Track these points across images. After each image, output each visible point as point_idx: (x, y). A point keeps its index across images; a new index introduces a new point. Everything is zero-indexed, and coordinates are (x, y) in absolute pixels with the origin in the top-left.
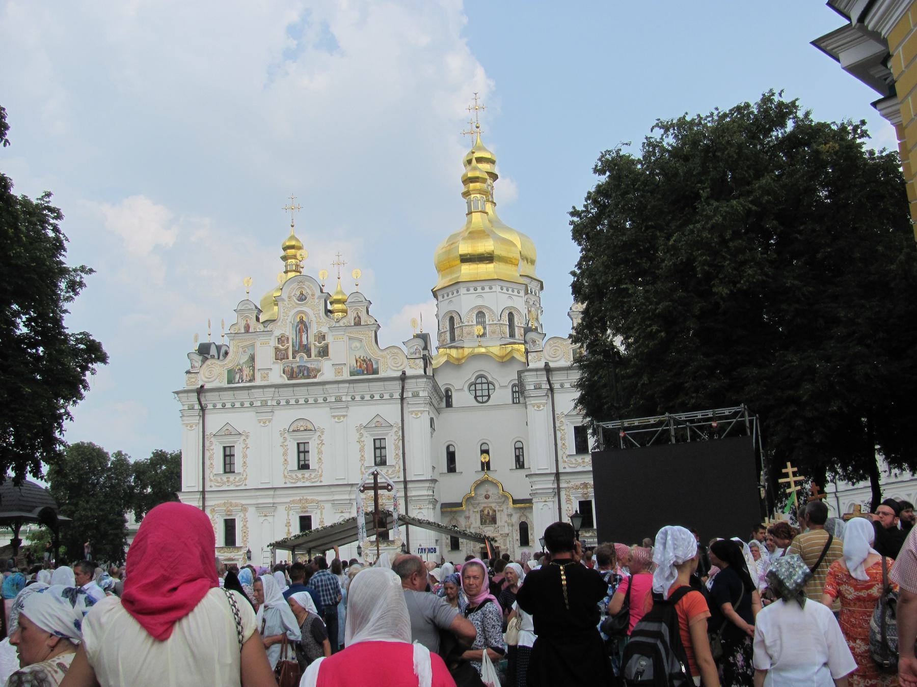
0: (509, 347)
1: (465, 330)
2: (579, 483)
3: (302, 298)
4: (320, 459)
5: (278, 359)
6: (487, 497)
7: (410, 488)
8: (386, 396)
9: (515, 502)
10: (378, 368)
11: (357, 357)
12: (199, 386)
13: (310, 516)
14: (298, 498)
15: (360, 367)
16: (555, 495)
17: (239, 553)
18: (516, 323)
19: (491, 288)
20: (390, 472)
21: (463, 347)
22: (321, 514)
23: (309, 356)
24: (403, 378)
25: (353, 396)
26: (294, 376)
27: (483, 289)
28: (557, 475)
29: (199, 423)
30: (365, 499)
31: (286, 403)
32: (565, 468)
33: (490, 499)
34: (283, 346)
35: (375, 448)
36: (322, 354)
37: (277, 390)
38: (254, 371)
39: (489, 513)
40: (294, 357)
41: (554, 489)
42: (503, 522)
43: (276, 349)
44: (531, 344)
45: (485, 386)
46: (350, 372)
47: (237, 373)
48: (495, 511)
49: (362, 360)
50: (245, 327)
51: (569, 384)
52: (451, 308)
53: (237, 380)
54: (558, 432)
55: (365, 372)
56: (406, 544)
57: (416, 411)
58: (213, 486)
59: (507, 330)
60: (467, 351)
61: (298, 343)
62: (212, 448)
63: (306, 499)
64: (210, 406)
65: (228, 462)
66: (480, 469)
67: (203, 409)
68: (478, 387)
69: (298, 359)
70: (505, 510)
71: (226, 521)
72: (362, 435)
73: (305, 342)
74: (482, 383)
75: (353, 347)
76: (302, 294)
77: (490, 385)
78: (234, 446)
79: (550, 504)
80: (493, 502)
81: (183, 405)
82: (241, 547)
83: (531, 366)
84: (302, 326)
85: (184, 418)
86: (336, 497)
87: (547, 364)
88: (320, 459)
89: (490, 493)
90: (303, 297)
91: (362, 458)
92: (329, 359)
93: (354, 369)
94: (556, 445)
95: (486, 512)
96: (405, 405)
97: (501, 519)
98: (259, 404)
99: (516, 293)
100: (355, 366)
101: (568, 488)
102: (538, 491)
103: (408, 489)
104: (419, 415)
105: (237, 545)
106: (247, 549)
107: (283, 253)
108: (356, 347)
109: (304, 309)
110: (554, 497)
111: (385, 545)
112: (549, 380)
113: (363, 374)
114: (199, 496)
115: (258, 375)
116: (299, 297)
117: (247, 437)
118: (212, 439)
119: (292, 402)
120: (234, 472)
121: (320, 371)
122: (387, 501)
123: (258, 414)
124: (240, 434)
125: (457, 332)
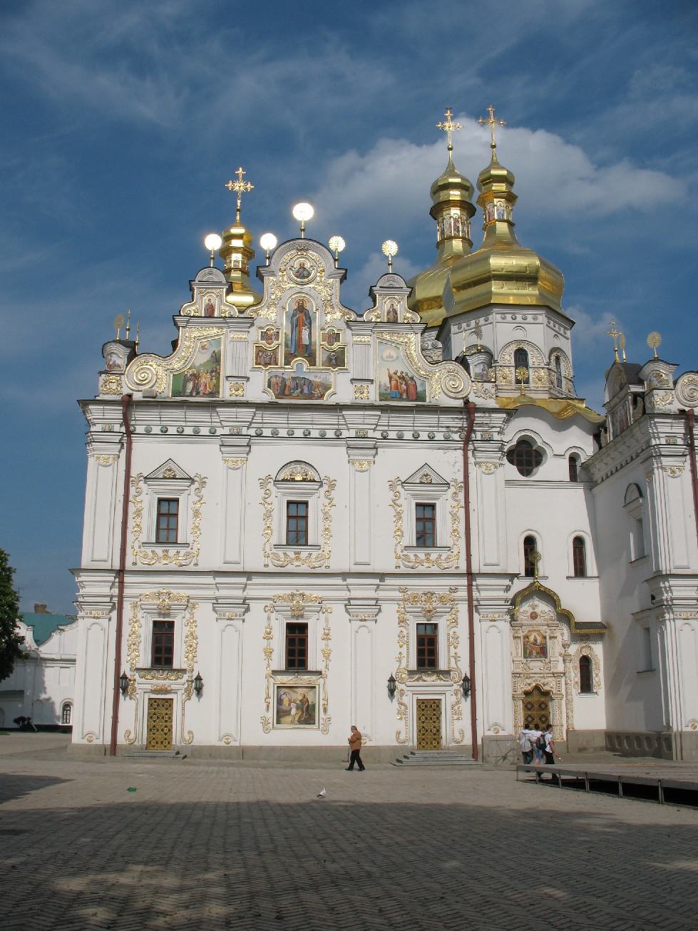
1: (499, 374)
5: (259, 364)
6: (534, 616)
10: (425, 391)
11: (392, 372)
13: (306, 625)
14: (289, 592)
15: (397, 388)
17: (179, 681)
22: (327, 620)
23: (313, 363)
24: (468, 409)
26: (287, 392)
29: (119, 457)
33: (538, 621)
36: (334, 361)
38: (218, 379)
39: (536, 640)
40: (288, 363)
42: (557, 654)
43: (260, 350)
46: (381, 394)
48: (545, 638)
49: (399, 377)
50: (206, 310)
55: (405, 397)
56: (469, 676)
59: (554, 378)
61: (294, 343)
62: (138, 499)
63: (303, 595)
64: (140, 429)
65: (163, 525)
67: (129, 433)
70: (560, 638)
71: (155, 623)
72: (397, 495)
73: (305, 341)
75: (385, 356)
76: (302, 267)
82: (184, 671)
84: (301, 316)
86: (354, 594)
88: (326, 529)
89: (538, 610)
91: (399, 533)
95: (532, 639)
96: (470, 453)
97: (555, 648)
98: (226, 431)
99: (562, 332)
105: (176, 665)
106: (195, 675)
108: (390, 357)
111: (434, 677)
113: (401, 399)
118: (142, 484)
121: (330, 388)
123: (223, 449)
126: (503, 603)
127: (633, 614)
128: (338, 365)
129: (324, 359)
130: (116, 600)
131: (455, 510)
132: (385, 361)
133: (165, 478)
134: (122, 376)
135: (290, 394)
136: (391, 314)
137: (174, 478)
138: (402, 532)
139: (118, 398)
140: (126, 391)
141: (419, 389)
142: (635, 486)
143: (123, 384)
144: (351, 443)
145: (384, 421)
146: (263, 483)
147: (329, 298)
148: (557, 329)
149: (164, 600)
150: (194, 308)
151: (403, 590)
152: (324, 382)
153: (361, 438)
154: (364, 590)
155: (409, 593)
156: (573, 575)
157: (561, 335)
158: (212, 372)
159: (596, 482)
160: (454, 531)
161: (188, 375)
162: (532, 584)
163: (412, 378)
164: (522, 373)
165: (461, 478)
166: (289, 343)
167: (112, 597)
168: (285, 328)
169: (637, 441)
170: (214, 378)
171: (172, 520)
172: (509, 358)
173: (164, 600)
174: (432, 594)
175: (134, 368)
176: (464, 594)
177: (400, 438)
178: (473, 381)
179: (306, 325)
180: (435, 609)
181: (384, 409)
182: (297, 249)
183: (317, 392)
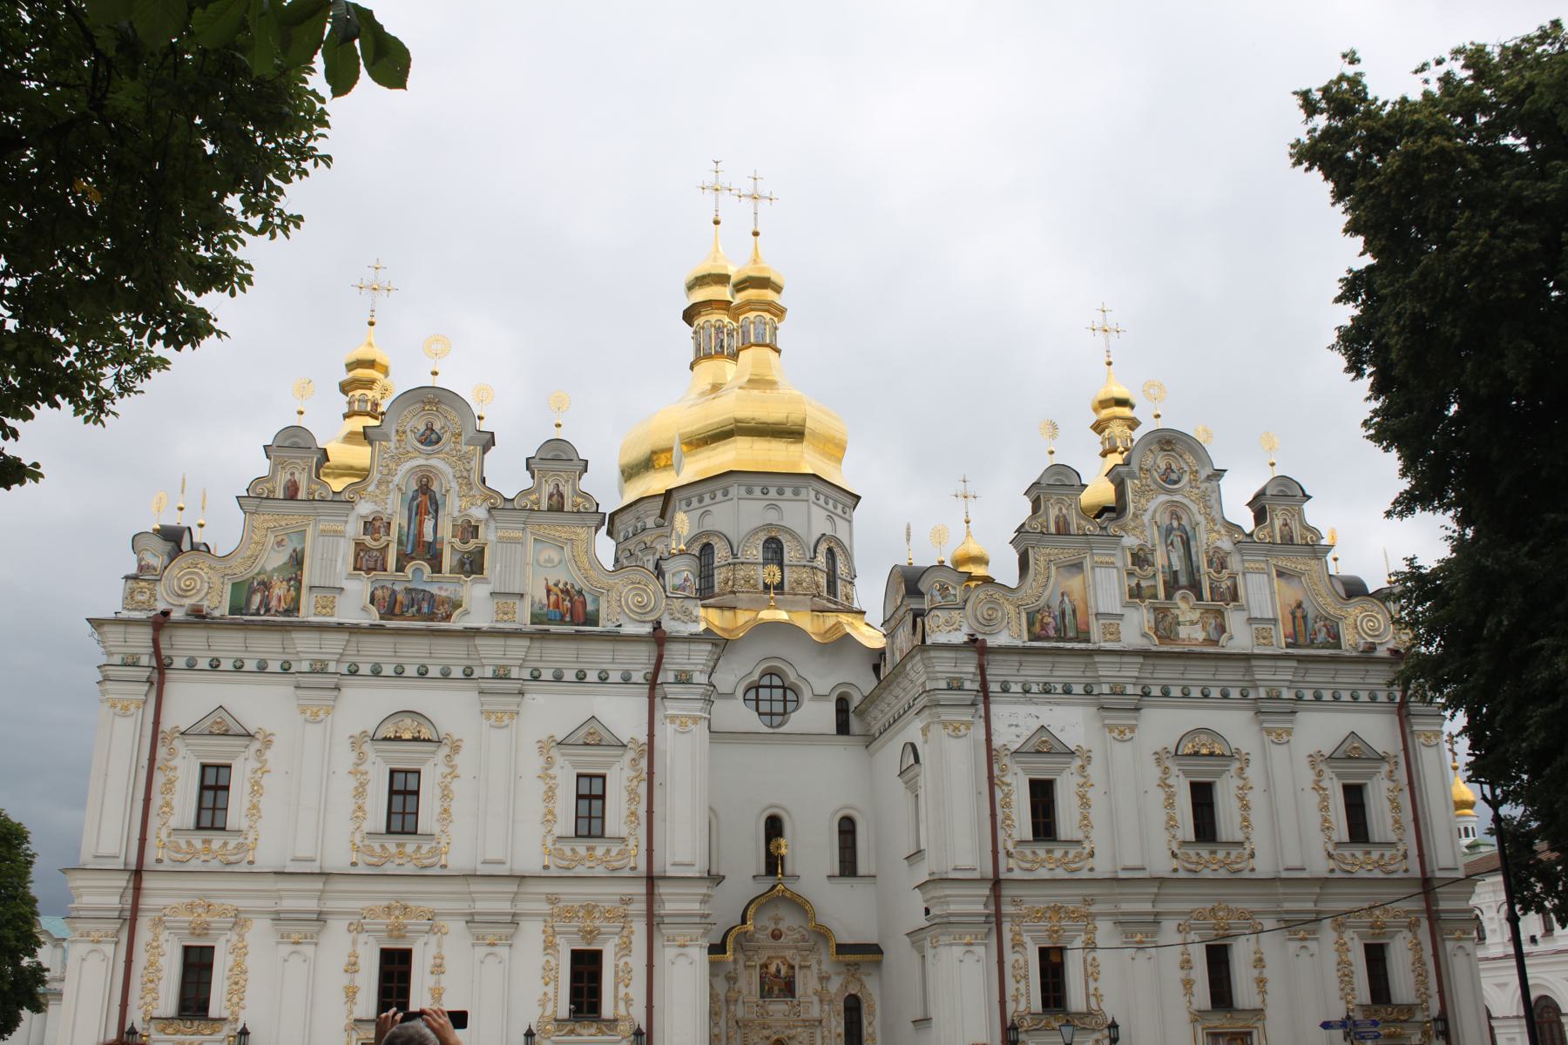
0: (831, 619)
2: (1043, 906)
3: (430, 438)
4: (445, 810)
5: (360, 569)
6: (776, 935)
7: (660, 895)
8: (615, 676)
9: (842, 949)
10: (598, 611)
11: (551, 584)
12: (159, 612)
14: (385, 903)
15: (557, 605)
16: (990, 929)
18: (839, 572)
19: (796, 493)
20: (614, 852)
21: (735, 608)
22: (439, 946)
24: (659, 638)
25: (536, 669)
26: (397, 611)
27: (780, 492)
28: (997, 883)
29: (145, 702)
30: (552, 915)
31: (372, 672)
32: (1010, 870)
34: (375, 540)
35: (579, 797)
36: (467, 566)
37: (354, 638)
38: (298, 589)
41: (988, 916)
43: (360, 546)
44: (936, 593)
45: (778, 693)
46: (533, 615)
47: (254, 591)
49: (562, 591)
50: (286, 488)
51: (1020, 685)
52: (710, 524)
53: (254, 607)
54: (996, 788)
55: (568, 619)
57: (686, 716)
58: (166, 860)
59: (822, 580)
60: (743, 617)
61: (411, 538)
62: (172, 764)
64: (179, 662)
66: (763, 870)
68: (764, 693)
69: (409, 568)
71: (187, 950)
72: (550, 762)
74: (771, 687)
75: (542, 560)
76: (430, 429)
77: (789, 693)
78: (229, 767)
79: (980, 950)
80: (789, 948)
81: (110, 654)
83: (941, 638)
84: (425, 499)
85: (109, 686)
86: (480, 906)
87: (973, 640)
88: (445, 810)
89: (783, 926)
90: (434, 437)
91: (550, 817)
92: (486, 581)
93: (541, 609)
94: (993, 815)
96: (658, 700)
98: (305, 667)
99: (839, 511)
100: (545, 601)
101: (1018, 916)
102: (952, 919)
103: (656, 898)
104: (691, 726)
107: (345, 376)
108: (550, 560)
109: (433, 462)
110: (987, 935)
112: (982, 669)
113: (562, 621)
114: (124, 884)
115: (306, 600)
116: (423, 435)
117: (268, 743)
118: (178, 743)
119: (388, 670)
120: (223, 829)
121: (461, 606)
122: (605, 924)
123: (300, 692)
124: (249, 735)
125: (719, 577)
126: (697, 920)
127: (907, 934)
128: (473, 572)
129: (455, 563)
130: (127, 914)
131: (635, 782)
132: (541, 566)
133: (211, 734)
134: (158, 583)
135: (402, 614)
136: (556, 496)
137: (225, 734)
138: (554, 816)
139: (152, 614)
140: (161, 606)
141: (590, 607)
142: (910, 748)
143: (158, 597)
144: (485, 685)
145: (535, 653)
146: (355, 743)
147: (465, 474)
148: (832, 509)
149: (199, 915)
150: (268, 485)
151: (552, 900)
152: (452, 596)
153: (501, 678)
154: (494, 902)
155: (561, 905)
156: (837, 871)
157: (836, 514)
158: (290, 579)
159: (874, 735)
160: (632, 813)
161: (255, 584)
162: (774, 887)
163: (580, 593)
164: (772, 574)
165: (644, 739)
166: (404, 538)
167: (122, 910)
168: (399, 520)
169: (912, 681)
170: (292, 589)
171: (220, 793)
172: (756, 552)
173: (199, 915)
174: (595, 907)
175: (177, 571)
176: (643, 906)
177: (558, 678)
178: (667, 596)
179: (429, 513)
180: (597, 928)
181: (531, 636)
182: (423, 402)
183: (441, 611)
